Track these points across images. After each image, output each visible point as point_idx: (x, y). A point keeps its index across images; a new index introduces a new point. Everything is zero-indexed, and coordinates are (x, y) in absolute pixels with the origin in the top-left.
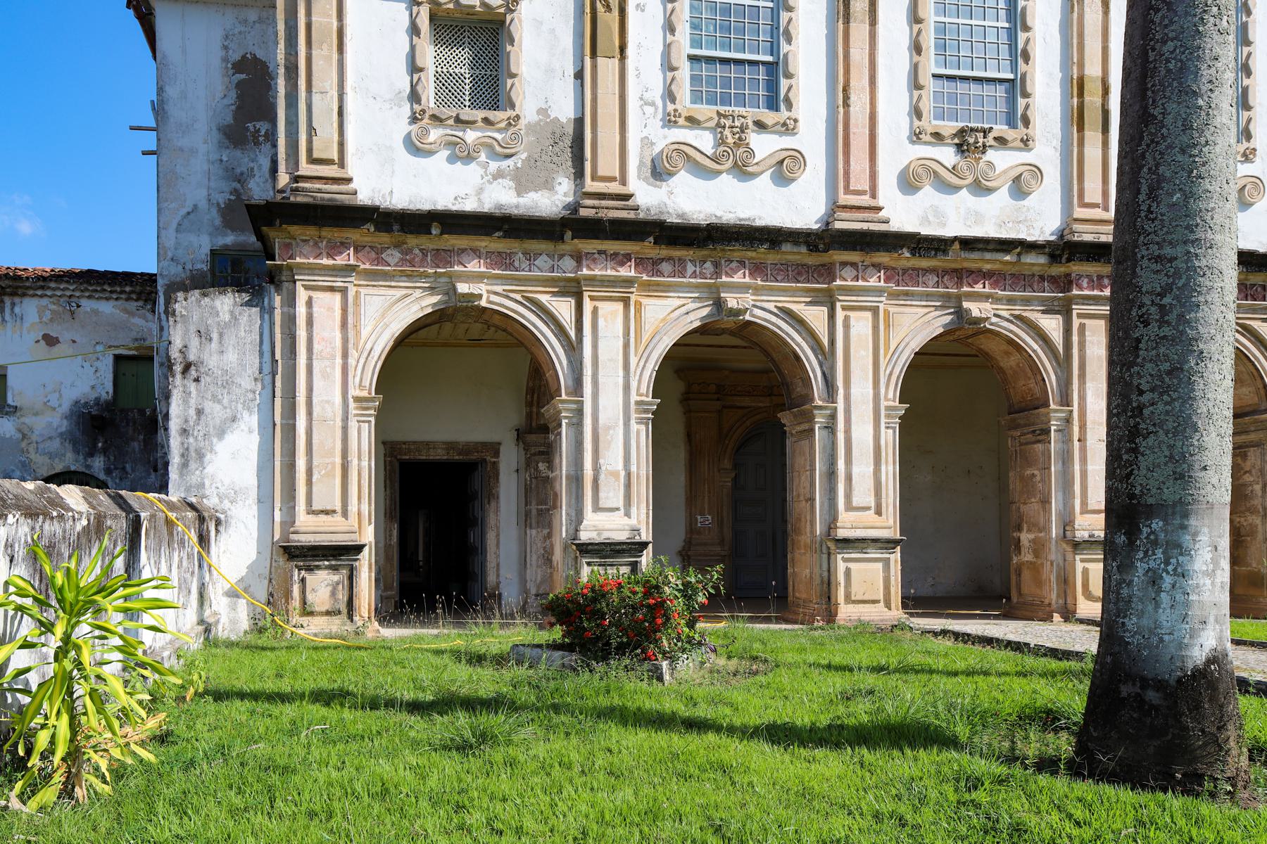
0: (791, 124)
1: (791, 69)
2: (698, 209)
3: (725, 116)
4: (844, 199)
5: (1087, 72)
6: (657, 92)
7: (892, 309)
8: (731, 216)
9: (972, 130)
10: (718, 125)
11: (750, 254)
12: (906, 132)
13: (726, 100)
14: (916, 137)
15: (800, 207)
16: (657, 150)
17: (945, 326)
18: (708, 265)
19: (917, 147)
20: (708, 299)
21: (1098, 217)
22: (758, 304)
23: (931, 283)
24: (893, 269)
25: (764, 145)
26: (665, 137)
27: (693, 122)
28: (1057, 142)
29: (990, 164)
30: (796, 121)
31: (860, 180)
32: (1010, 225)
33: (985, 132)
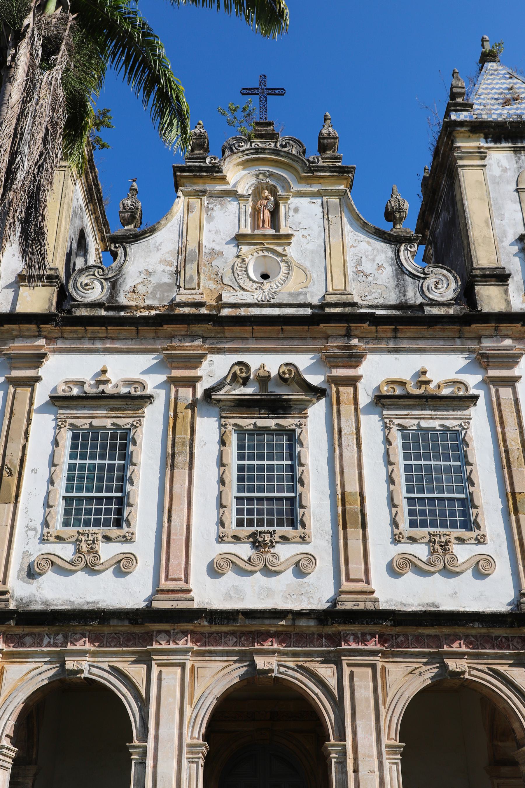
0: (129, 536)
1: (131, 501)
4: (164, 584)
5: (347, 489)
6: (38, 523)
7: (197, 665)
8: (82, 600)
9: (261, 533)
10: (77, 540)
11: (88, 628)
12: (215, 536)
13: (87, 523)
14: (221, 539)
15: (130, 593)
16: (33, 559)
17: (241, 676)
18: (60, 637)
20: (56, 662)
21: (359, 589)
22: (95, 664)
23: (231, 643)
24: (202, 633)
25: (107, 552)
26: (40, 550)
27: (60, 539)
28: (329, 537)
29: (276, 555)
30: (132, 534)
32: (295, 596)
33: (272, 534)
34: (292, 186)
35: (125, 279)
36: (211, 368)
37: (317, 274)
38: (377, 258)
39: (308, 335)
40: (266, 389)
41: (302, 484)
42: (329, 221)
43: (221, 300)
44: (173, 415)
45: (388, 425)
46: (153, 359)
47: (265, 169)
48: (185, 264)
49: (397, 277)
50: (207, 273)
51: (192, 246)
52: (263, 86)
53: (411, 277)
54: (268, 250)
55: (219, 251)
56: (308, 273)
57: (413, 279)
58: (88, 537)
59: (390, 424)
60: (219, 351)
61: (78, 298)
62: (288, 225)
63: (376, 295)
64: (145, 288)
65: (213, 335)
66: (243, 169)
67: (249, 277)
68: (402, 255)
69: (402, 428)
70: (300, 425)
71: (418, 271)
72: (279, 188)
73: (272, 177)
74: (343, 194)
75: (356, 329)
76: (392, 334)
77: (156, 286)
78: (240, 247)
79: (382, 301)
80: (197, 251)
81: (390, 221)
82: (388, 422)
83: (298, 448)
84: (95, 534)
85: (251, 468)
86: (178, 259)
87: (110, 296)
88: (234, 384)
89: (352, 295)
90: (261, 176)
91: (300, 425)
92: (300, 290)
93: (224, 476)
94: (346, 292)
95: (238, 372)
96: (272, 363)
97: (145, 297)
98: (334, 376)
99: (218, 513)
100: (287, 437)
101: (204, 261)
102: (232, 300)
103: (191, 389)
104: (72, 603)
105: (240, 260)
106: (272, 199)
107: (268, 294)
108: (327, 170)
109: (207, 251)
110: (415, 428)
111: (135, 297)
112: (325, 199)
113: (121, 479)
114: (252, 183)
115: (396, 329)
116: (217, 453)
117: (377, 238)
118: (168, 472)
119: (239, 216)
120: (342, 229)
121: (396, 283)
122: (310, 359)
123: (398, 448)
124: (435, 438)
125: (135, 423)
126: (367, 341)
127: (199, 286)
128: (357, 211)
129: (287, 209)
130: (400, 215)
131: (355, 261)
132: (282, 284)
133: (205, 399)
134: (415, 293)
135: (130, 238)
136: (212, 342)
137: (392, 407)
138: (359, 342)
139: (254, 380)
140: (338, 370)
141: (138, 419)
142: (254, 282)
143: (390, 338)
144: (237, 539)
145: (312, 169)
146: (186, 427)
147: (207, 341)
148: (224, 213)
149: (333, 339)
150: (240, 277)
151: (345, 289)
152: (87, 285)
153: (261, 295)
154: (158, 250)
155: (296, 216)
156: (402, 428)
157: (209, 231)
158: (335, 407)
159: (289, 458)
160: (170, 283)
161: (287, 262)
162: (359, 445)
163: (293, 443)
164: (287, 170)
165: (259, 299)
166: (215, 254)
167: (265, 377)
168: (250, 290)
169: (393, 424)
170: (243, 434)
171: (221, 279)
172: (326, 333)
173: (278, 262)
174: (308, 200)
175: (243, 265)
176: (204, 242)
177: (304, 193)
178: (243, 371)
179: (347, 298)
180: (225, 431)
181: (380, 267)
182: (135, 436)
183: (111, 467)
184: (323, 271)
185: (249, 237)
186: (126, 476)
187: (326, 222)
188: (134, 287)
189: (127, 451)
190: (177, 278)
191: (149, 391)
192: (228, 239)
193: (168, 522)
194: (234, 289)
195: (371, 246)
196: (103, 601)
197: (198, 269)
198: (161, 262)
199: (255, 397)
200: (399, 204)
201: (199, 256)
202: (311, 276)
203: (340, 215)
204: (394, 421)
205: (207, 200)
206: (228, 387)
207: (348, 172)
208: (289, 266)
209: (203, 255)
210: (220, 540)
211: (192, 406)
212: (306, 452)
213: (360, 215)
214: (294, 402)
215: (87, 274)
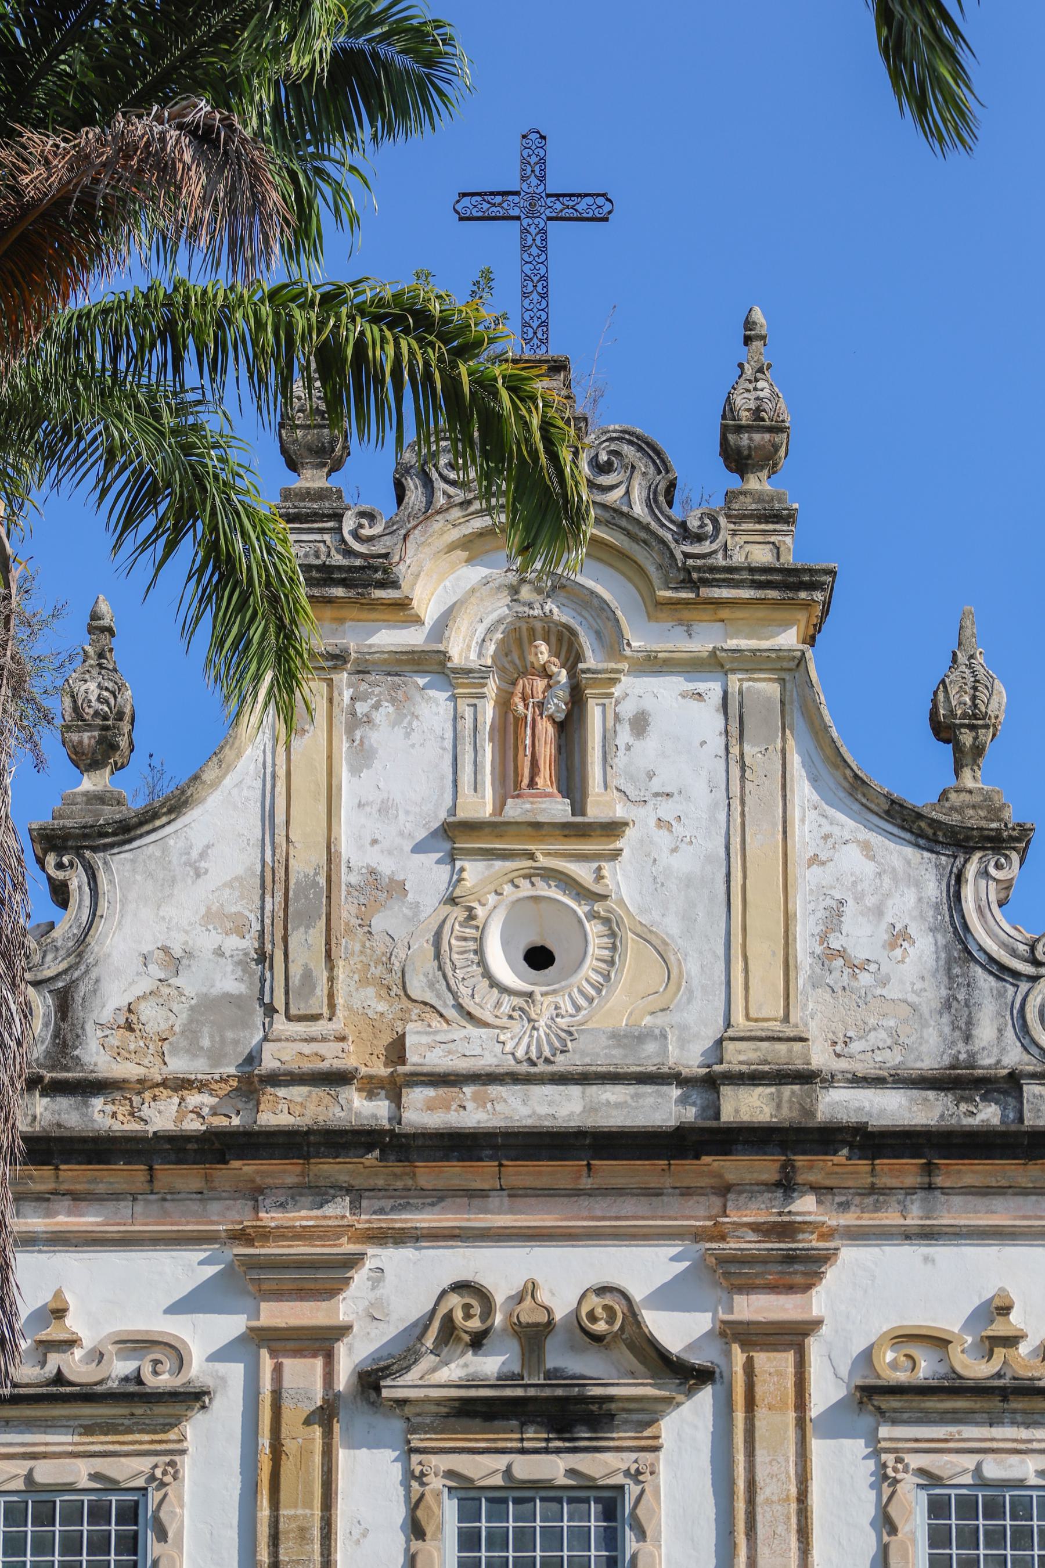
34: (628, 634)
36: (378, 1293)
37: (699, 964)
38: (890, 903)
39: (668, 1182)
40: (541, 1360)
43: (402, 1060)
44: (272, 1446)
45: (890, 1472)
46: (201, 1263)
48: (286, 928)
49: (949, 970)
50: (356, 959)
51: (306, 862)
52: (534, 181)
53: (991, 973)
54: (549, 875)
55: (391, 880)
56: (672, 959)
57: (999, 978)
59: (895, 1470)
60: (400, 1238)
62: (613, 782)
63: (880, 1037)
64: (163, 1012)
65: (380, 1183)
66: (469, 561)
67: (487, 974)
68: (968, 892)
69: (930, 1479)
71: (1014, 953)
74: (792, 665)
75: (811, 1168)
76: (919, 1180)
77: (197, 1005)
78: (458, 864)
79: (899, 1059)
80: (322, 881)
81: (947, 741)
82: (891, 1463)
83: (631, 1544)
86: (263, 908)
88: (446, 1350)
91: (638, 1472)
92: (647, 1020)
94: (790, 1032)
95: (458, 1315)
96: (558, 1275)
97: (166, 1047)
98: (740, 1323)
100: (600, 1506)
101: (344, 914)
102: (438, 1060)
103: (319, 1363)
105: (459, 913)
106: (563, 676)
107: (547, 1035)
108: (743, 581)
109: (354, 879)
110: (968, 1479)
111: (132, 1046)
112: (734, 679)
114: (495, 616)
115: (929, 1164)
117: (896, 831)
119: (455, 747)
120: (784, 797)
121: (944, 992)
123: (914, 1541)
124: (1022, 1508)
126: (843, 1199)
127: (332, 1006)
128: (835, 734)
129: (610, 723)
130: (976, 738)
131: (821, 914)
132: (591, 1000)
133: (363, 1392)
134: (1000, 1031)
136: (377, 1204)
137: (906, 1416)
138: (819, 1202)
139: (504, 1330)
140: (753, 1297)
142: (504, 990)
143: (911, 1191)
145: (695, 575)
146: (308, 1484)
147: (365, 1203)
148: (407, 735)
149: (743, 1198)
150: (460, 974)
151: (786, 1019)
153: (526, 1039)
154: (198, 875)
155: (638, 745)
156: (930, 1479)
157: (360, 805)
158: (740, 1416)
160: (240, 997)
161: (607, 921)
162: (804, 1534)
163: (618, 1524)
164: (611, 566)
165: (520, 1053)
166: (382, 888)
167: (537, 1325)
168: (490, 1019)
169: (906, 1470)
170: (473, 1499)
171: (399, 982)
172: (720, 1176)
173: (580, 921)
174: (676, 683)
175: (470, 932)
176: (346, 848)
177: (666, 661)
178: (472, 1311)
179: (790, 1051)
180: (422, 1495)
181: (899, 937)
184: (721, 951)
185: (487, 830)
187: (735, 771)
188: (130, 1011)
190: (262, 980)
191: (198, 1369)
192: (421, 834)
194: (441, 1015)
195: (872, 858)
197: (328, 943)
198: (211, 918)
199: (508, 1392)
200: (974, 698)
201: (329, 897)
202: (681, 972)
203: (779, 746)
204: (908, 1458)
205: (349, 686)
206: (428, 1361)
207: (812, 586)
208: (613, 935)
209: (344, 893)
211: (325, 1415)
212: (652, 1555)
213: (843, 750)
214: (620, 1405)
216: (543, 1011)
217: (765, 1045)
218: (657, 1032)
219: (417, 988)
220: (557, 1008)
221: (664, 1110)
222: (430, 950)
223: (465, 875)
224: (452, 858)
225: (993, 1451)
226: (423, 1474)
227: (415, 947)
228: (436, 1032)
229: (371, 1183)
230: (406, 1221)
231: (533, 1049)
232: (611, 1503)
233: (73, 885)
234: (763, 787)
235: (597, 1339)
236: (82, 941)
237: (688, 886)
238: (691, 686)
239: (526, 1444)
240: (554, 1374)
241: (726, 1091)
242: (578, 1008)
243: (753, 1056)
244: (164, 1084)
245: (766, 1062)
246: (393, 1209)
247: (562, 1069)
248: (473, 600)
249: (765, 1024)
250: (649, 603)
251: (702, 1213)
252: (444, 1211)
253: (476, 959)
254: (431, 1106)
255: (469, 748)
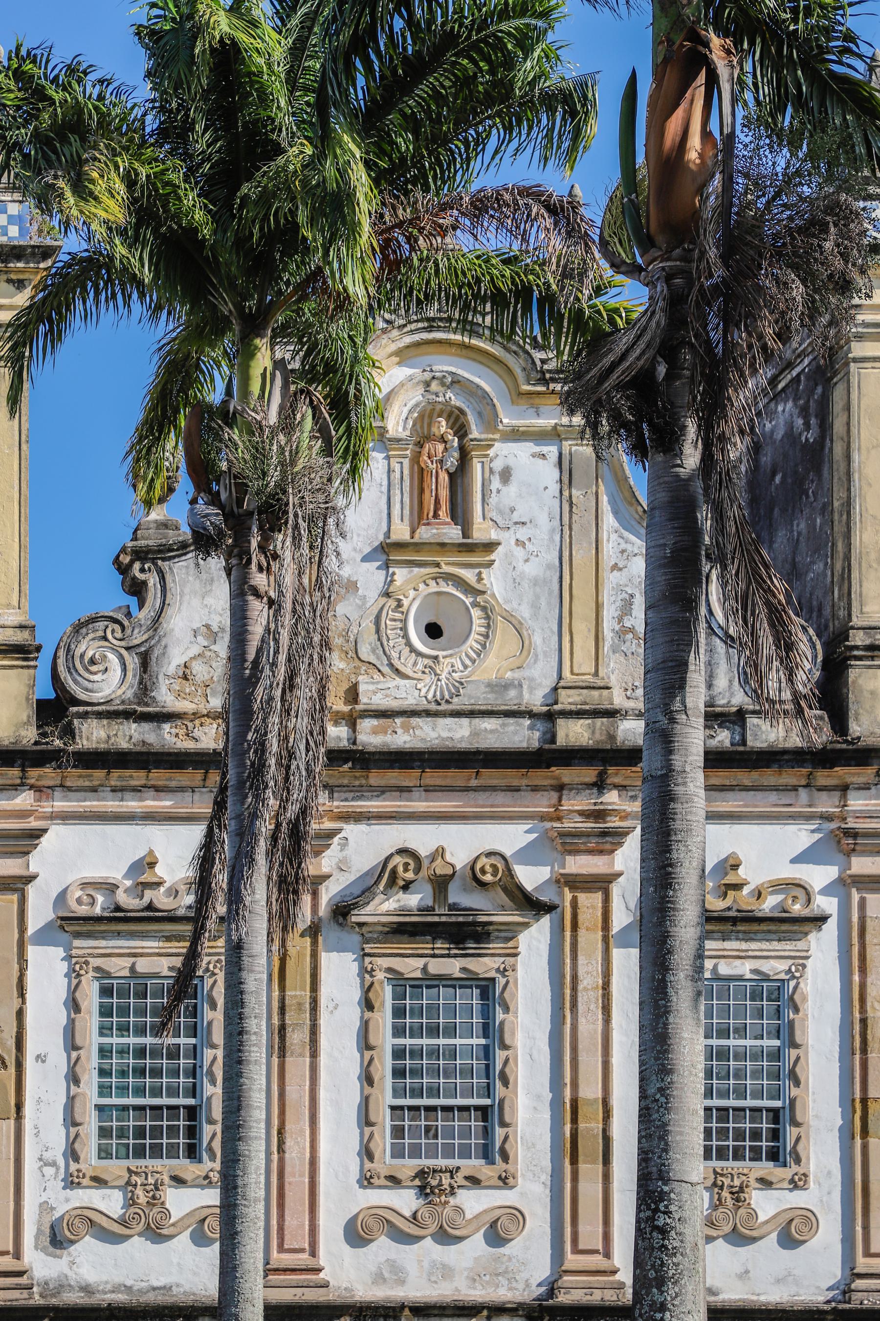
2: (105, 1278)
3: (136, 1173)
6: (57, 1152)
8: (144, 1284)
10: (128, 1183)
13: (140, 1152)
14: (367, 1181)
19: (369, 1191)
26: (67, 1200)
27: (99, 1182)
31: (297, 1236)
35: (166, 647)
36: (344, 853)
37: (542, 637)
39: (524, 782)
40: (446, 898)
41: (505, 1082)
42: (571, 504)
47: (446, 368)
55: (348, 580)
56: (525, 633)
58: (146, 1179)
61: (82, 696)
62: (489, 515)
65: (346, 782)
66: (399, 364)
67: (409, 644)
70: (505, 970)
72: (471, 418)
73: (456, 386)
78: (391, 570)
83: (500, 1016)
84: (157, 1173)
85: (416, 1053)
87: (139, 689)
89: (608, 688)
90: (434, 387)
91: (505, 970)
92: (509, 675)
93: (372, 1069)
97: (208, 691)
99: (362, 1134)
102: (380, 701)
104: (129, 1289)
111: (187, 690)
113: (193, 1072)
114: (413, 402)
116: (358, 1024)
118: (275, 1060)
119: (389, 491)
122: (526, 832)
125: (211, 967)
132: (474, 661)
135: (173, 550)
141: (216, 958)
142: (419, 654)
144: (394, 1181)
146: (303, 975)
147: (336, 795)
150: (391, 644)
152: (92, 661)
153: (433, 687)
155: (504, 490)
158: (568, 934)
159: (481, 1032)
161: (484, 609)
165: (430, 696)
167: (445, 875)
168: (411, 674)
171: (353, 648)
173: (467, 609)
175: (398, 616)
179: (600, 696)
180: (372, 984)
182: (214, 993)
183: (174, 1053)
186: (201, 1067)
187: (566, 507)
188: (185, 666)
189: (198, 1020)
192: (367, 550)
193: (279, 1153)
196: (178, 1286)
202: (530, 643)
208: (488, 618)
210: (366, 1183)
212: (513, 1022)
215: (91, 636)
216: (444, 670)
217: (585, 691)
218: (516, 682)
219: (365, 652)
220: (452, 666)
221: (521, 736)
222: (373, 627)
223: (396, 577)
224: (387, 566)
225: (724, 957)
226: (373, 970)
227: (363, 625)
228: (378, 683)
229: (340, 782)
230: (361, 807)
231: (438, 693)
232: (486, 988)
233: (151, 583)
234: (583, 518)
235: (482, 884)
236: (157, 621)
237: (535, 585)
238: (537, 449)
239: (436, 952)
240: (453, 907)
241: (561, 722)
242: (466, 667)
243: (577, 699)
244: (207, 716)
245: (585, 703)
246: (353, 799)
247: (458, 707)
248: (402, 391)
249: (583, 677)
250: (513, 393)
251: (546, 803)
252: (384, 800)
253: (401, 633)
254: (375, 731)
255: (398, 492)
